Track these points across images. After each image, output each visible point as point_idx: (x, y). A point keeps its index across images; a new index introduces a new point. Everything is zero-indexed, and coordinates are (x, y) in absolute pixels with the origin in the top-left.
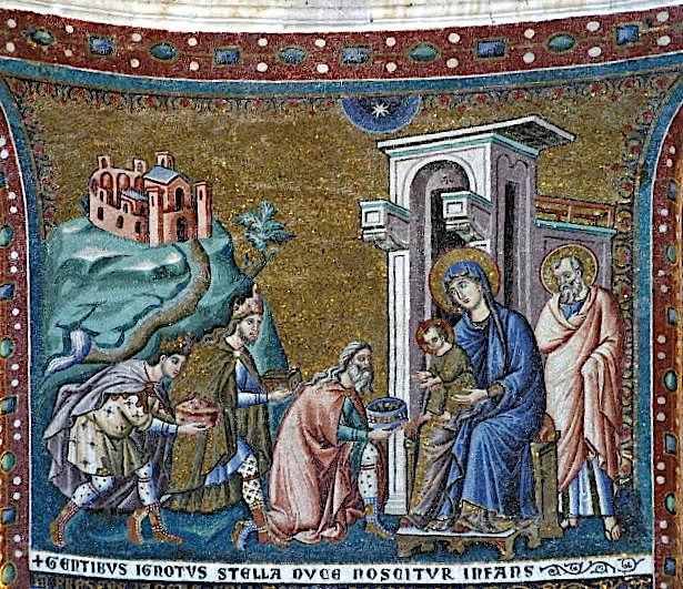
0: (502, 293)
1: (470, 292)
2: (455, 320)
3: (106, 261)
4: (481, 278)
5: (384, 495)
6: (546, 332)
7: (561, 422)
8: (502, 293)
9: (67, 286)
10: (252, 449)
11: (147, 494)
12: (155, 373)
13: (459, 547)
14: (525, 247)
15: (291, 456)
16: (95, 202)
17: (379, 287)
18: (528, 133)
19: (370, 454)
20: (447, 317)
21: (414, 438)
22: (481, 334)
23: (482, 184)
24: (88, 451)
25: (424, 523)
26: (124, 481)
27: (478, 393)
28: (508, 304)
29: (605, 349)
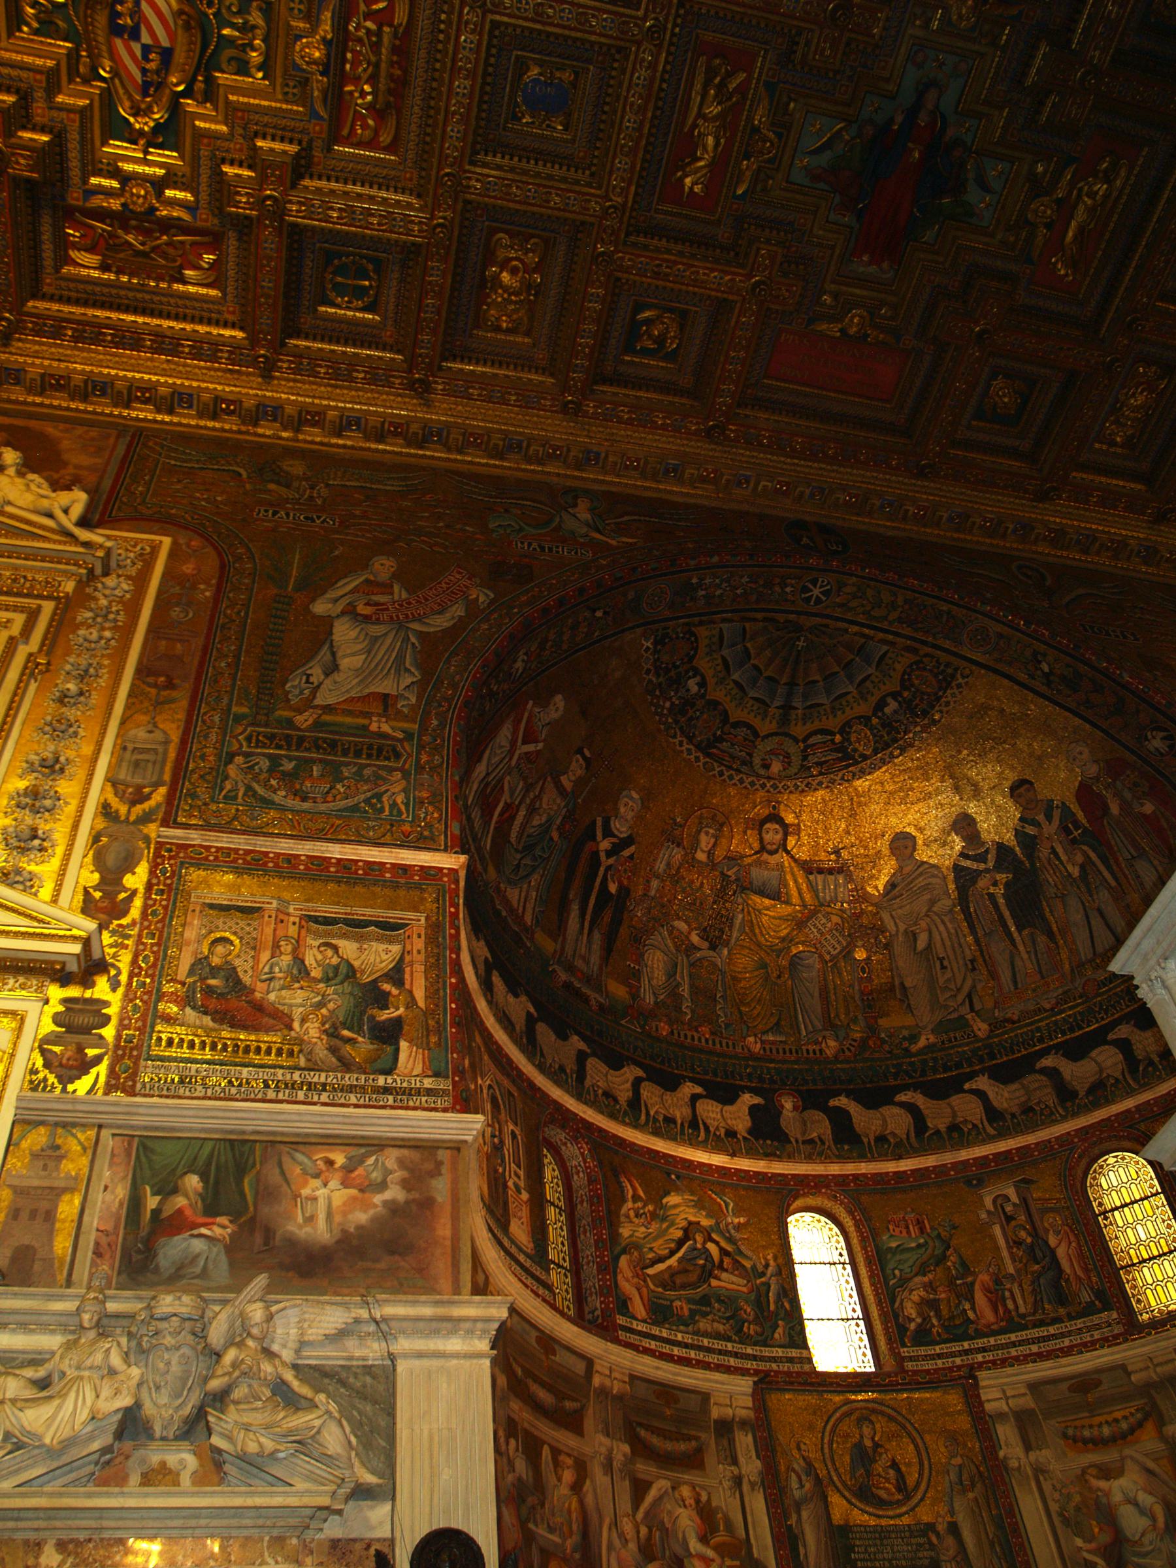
0: (1034, 1233)
1: (1023, 1234)
2: (1021, 1244)
3: (898, 1246)
4: (1025, 1229)
5: (1017, 1307)
6: (1052, 1241)
7: (1068, 1271)
8: (1034, 1233)
9: (889, 1256)
10: (967, 1299)
11: (935, 1321)
12: (926, 1279)
13: (1048, 1321)
14: (1036, 1217)
15: (980, 1298)
16: (891, 1227)
17: (993, 1238)
18: (1024, 1181)
19: (1007, 1294)
20: (1019, 1243)
21: (1020, 1285)
22: (1032, 1246)
23: (1014, 1198)
24: (911, 1310)
25: (1034, 1314)
26: (926, 1319)
27: (1037, 1267)
28: (1037, 1234)
29: (1074, 1244)
